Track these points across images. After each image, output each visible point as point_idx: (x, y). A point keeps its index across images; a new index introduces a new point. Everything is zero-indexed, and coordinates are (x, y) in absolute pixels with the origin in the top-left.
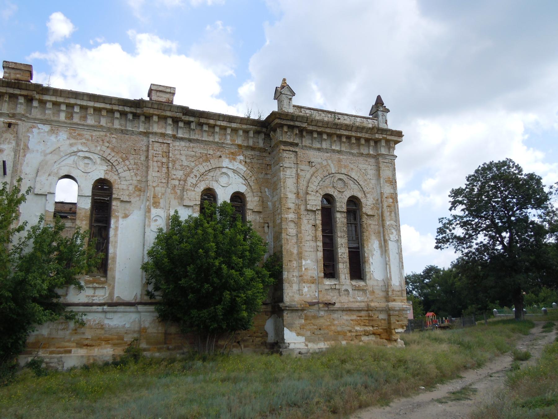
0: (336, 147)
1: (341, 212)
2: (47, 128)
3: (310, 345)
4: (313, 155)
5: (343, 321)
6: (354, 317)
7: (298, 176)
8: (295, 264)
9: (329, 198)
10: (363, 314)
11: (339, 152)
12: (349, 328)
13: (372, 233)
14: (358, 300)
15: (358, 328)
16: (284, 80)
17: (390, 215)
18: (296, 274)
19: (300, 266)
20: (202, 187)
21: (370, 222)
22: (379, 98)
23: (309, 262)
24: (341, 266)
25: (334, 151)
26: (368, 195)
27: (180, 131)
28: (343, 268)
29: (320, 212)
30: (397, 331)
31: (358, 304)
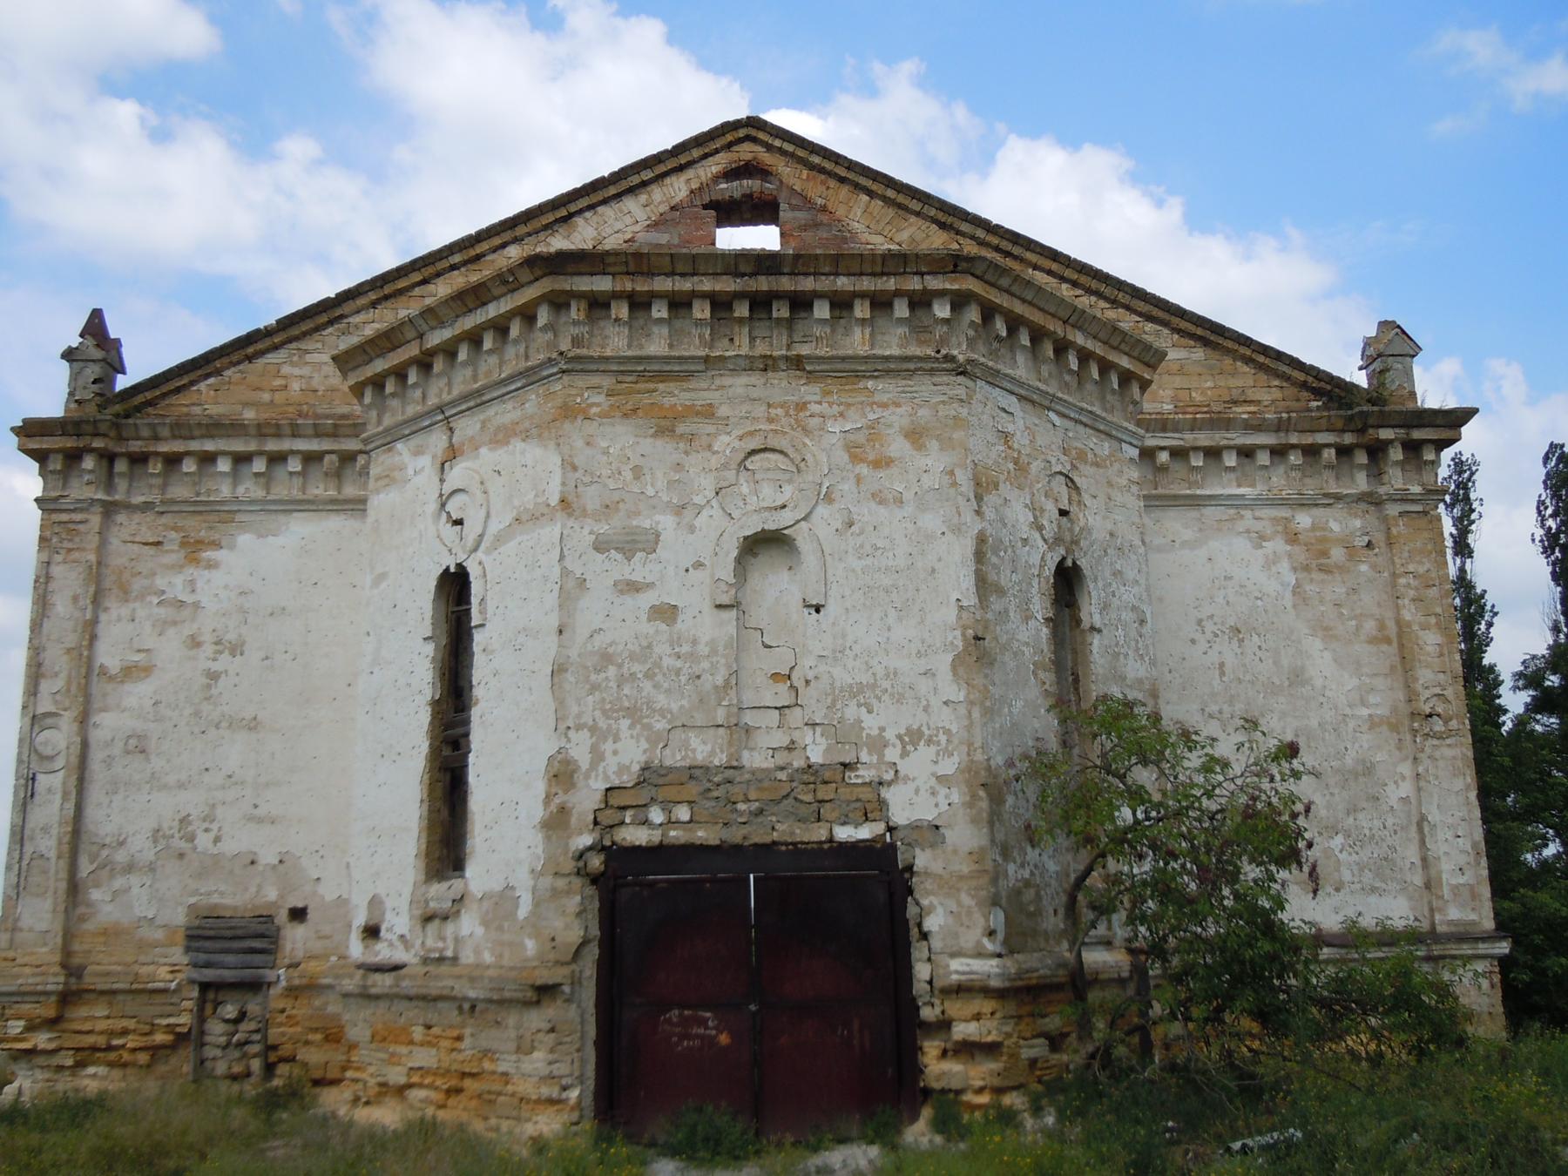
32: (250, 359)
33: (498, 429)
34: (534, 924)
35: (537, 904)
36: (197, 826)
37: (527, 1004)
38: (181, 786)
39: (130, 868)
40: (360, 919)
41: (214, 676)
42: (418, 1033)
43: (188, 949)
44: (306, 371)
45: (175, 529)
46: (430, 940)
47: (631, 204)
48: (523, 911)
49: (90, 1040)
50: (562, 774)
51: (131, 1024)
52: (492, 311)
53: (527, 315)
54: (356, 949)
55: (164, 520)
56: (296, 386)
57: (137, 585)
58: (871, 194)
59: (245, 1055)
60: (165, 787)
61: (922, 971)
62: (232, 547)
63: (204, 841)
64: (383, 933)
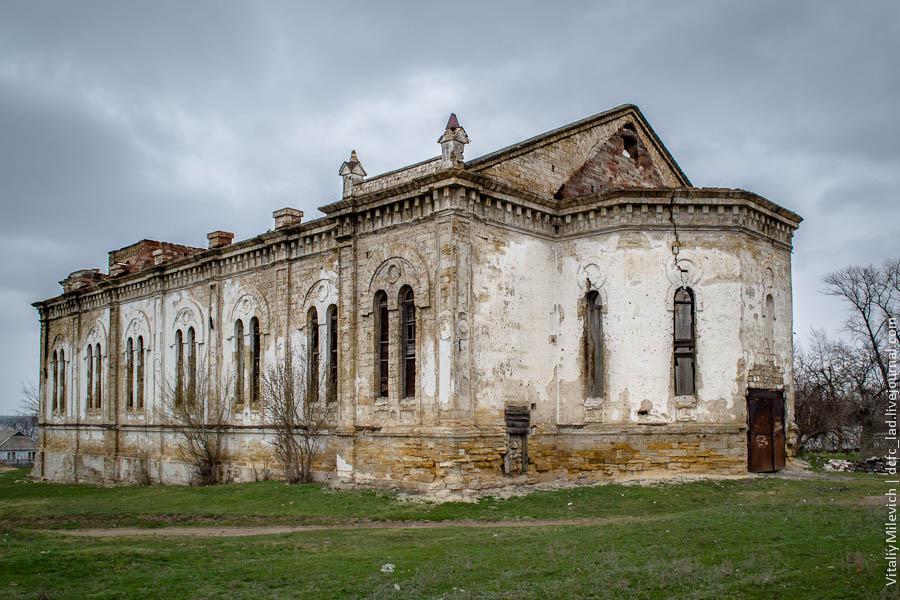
2: (229, 281)
3: (359, 476)
4: (370, 243)
7: (355, 275)
10: (411, 441)
11: (395, 227)
14: (403, 423)
15: (406, 459)
16: (354, 152)
17: (445, 302)
19: (353, 386)
21: (426, 316)
23: (363, 379)
25: (407, 224)
26: (421, 280)
27: (294, 251)
28: (394, 384)
30: (442, 465)
31: (403, 429)
34: (734, 410)
35: (735, 404)
36: (505, 368)
38: (500, 351)
39: (487, 385)
40: (638, 408)
41: (506, 303)
42: (675, 445)
43: (506, 420)
45: (493, 234)
46: (681, 415)
47: (605, 128)
50: (741, 364)
51: (490, 450)
52: (714, 201)
53: (728, 208)
54: (635, 418)
55: (487, 228)
56: (522, 176)
57: (482, 256)
58: (657, 149)
59: (517, 462)
62: (509, 246)
63: (508, 374)
64: (652, 412)
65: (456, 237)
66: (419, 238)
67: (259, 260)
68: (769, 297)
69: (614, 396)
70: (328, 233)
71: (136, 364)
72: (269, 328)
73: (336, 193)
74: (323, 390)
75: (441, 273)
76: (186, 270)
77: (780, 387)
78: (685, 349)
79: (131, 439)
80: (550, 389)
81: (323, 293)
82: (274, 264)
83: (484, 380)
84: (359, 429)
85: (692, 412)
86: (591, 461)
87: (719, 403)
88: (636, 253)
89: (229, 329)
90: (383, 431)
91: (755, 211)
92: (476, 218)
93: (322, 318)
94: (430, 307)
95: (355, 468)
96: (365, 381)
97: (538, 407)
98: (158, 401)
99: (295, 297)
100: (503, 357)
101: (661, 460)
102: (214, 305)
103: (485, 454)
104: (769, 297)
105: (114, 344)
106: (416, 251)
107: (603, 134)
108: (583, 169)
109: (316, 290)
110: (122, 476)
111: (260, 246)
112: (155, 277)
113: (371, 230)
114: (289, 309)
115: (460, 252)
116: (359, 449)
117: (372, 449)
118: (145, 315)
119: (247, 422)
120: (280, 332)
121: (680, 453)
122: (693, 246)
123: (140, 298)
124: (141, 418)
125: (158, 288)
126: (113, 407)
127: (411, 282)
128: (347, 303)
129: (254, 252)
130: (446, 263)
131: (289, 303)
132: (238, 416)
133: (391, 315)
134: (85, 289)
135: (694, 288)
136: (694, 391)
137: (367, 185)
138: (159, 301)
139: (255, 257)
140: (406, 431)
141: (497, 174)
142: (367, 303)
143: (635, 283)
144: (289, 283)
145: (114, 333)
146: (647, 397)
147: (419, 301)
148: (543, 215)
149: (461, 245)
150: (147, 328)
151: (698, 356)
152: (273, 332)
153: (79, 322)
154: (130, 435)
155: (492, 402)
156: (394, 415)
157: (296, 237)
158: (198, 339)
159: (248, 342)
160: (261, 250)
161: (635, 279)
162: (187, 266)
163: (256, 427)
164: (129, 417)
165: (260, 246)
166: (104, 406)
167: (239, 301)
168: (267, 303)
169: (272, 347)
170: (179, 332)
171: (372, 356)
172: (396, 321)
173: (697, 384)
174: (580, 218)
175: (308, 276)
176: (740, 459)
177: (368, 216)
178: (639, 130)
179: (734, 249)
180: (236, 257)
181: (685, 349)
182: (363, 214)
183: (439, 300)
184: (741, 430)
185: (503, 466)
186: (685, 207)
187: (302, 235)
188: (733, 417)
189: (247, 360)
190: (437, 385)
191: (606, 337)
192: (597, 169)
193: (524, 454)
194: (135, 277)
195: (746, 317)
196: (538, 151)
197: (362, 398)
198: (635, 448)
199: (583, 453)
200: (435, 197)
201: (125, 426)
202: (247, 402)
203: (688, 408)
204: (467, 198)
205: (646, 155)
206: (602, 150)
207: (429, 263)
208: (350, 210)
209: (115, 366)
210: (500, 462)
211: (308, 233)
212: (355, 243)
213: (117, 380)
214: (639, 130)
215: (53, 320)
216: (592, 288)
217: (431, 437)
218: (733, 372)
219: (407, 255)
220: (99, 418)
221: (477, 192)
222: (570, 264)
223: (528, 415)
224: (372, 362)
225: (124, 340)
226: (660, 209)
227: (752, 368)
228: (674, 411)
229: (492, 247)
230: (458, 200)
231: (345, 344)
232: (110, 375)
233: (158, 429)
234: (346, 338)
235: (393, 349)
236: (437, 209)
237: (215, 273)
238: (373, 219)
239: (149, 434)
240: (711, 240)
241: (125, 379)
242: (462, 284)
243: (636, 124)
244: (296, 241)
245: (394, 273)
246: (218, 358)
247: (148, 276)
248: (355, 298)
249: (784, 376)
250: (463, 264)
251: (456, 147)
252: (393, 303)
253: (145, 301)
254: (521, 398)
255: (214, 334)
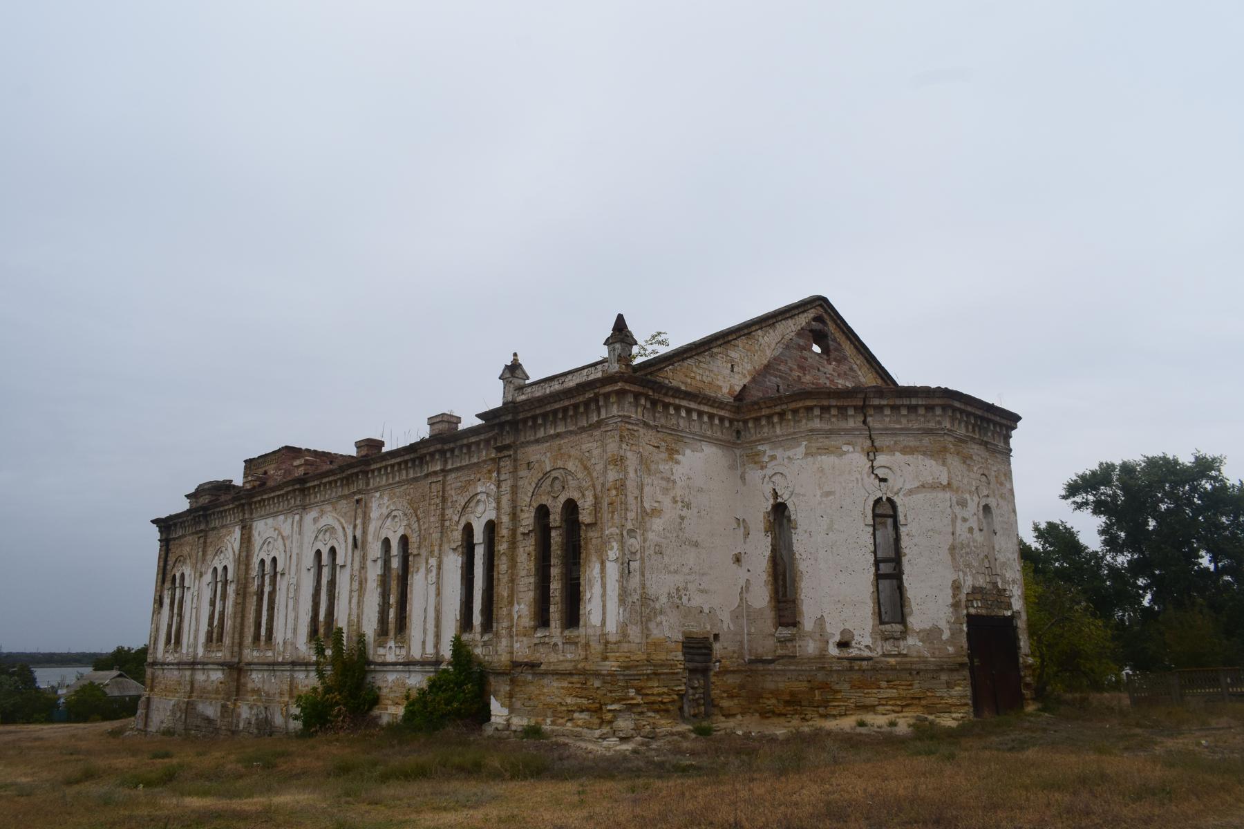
0: (561, 429)
1: (555, 528)
2: (378, 494)
5: (553, 689)
6: (565, 684)
7: (514, 489)
8: (504, 611)
9: (543, 512)
10: (575, 679)
11: (558, 435)
12: (559, 700)
13: (593, 552)
14: (567, 657)
15: (569, 700)
16: (515, 355)
18: (505, 625)
19: (510, 614)
20: (463, 523)
22: (620, 319)
24: (552, 609)
25: (571, 432)
26: (586, 493)
27: (450, 462)
29: (532, 534)
32: (683, 360)
33: (905, 447)
34: (951, 641)
35: (952, 634)
36: (682, 592)
37: (952, 670)
40: (837, 638)
41: (682, 518)
42: (884, 684)
43: (684, 654)
44: (701, 371)
46: (888, 647)
47: (791, 322)
48: (946, 635)
49: (652, 698)
50: (956, 587)
51: (665, 690)
52: (914, 402)
54: (833, 651)
55: (660, 435)
57: (653, 467)
60: (670, 572)
61: (1021, 660)
63: (685, 599)
64: (853, 643)
65: (624, 446)
66: (584, 447)
67: (411, 471)
68: (987, 509)
69: (808, 624)
70: (487, 442)
71: (267, 589)
72: (419, 548)
73: (494, 398)
74: (477, 619)
75: (608, 485)
76: (330, 483)
77: (1009, 613)
78: (889, 570)
79: (256, 678)
80: (736, 616)
81: (481, 508)
82: (427, 476)
83: (658, 607)
84: (515, 664)
85: (902, 643)
86: (787, 703)
87: (931, 634)
88: (827, 460)
89: (375, 550)
90: (543, 667)
91: (962, 412)
92: (646, 425)
93: (479, 537)
94: (595, 524)
95: (511, 712)
96: (523, 609)
97: (721, 638)
98: (289, 635)
99: (449, 512)
100: (678, 580)
101: (868, 701)
102: (359, 522)
103: (659, 695)
104: (987, 509)
105: (243, 567)
106: (581, 461)
107: (789, 328)
108: (767, 367)
109: (472, 504)
110: (241, 726)
111: (412, 456)
112: (294, 490)
113: (532, 438)
114: (443, 525)
115: (628, 462)
116: (517, 689)
117: (533, 689)
118: (280, 533)
119: (391, 658)
120: (432, 552)
121: (893, 693)
122: (891, 451)
123: (275, 515)
124: (270, 654)
125: (298, 502)
126: (237, 641)
127: (575, 495)
128: (505, 519)
129: (406, 462)
130: (612, 475)
131: (443, 518)
132: (381, 651)
133: (553, 533)
134: (214, 504)
135: (895, 499)
136: (903, 620)
137: (529, 390)
138: (297, 517)
139: (392, 472)
140: (568, 667)
141: (674, 377)
142: (528, 519)
143: (828, 494)
144: (443, 497)
145: (244, 554)
146: (847, 627)
147: (585, 517)
148: (722, 419)
149: (629, 454)
150: (281, 548)
151: (904, 577)
152: (424, 552)
153: (205, 542)
154: (254, 675)
155: (669, 629)
156: (556, 648)
157: (452, 445)
158: (339, 561)
159: (395, 563)
160: (413, 460)
161: (826, 489)
162: (331, 478)
163: (400, 664)
164: (255, 653)
165: (412, 456)
166: (227, 640)
167: (387, 517)
168: (418, 520)
169: (422, 570)
170: (319, 553)
171: (532, 580)
172: (559, 539)
173: (907, 610)
174: (764, 422)
175: (463, 489)
176: (963, 701)
177: (530, 423)
178: (829, 322)
179: (939, 454)
180: (386, 467)
181: (889, 570)
182: (525, 421)
183: (606, 516)
184: (962, 665)
185: (681, 709)
186: (880, 408)
187: (459, 443)
188: (951, 649)
189: (394, 585)
190: (604, 614)
191: (797, 556)
192: (782, 367)
193: (707, 694)
194: (273, 489)
195: (958, 532)
196: (715, 350)
197: (520, 628)
198: (837, 687)
199: (776, 693)
200: (601, 403)
201: (249, 664)
202: (392, 634)
203: (898, 639)
204: (637, 404)
205: (839, 348)
206: (787, 347)
207: (595, 474)
208: (509, 418)
209: (242, 593)
210: (679, 704)
211: (465, 441)
212: (516, 452)
213: (243, 611)
214: (829, 322)
215: (175, 539)
216: (780, 500)
217: (597, 674)
218: (947, 597)
219: (571, 466)
220: (219, 654)
221: (647, 397)
222: (754, 475)
223: (710, 649)
224: (532, 587)
225: (255, 562)
226: (851, 412)
227: (969, 591)
228: (879, 643)
229: (664, 456)
230: (626, 405)
231: (502, 565)
232: (236, 604)
233: (287, 667)
234: (504, 559)
235: (555, 571)
236: (603, 415)
237: (361, 484)
238: (535, 427)
239: (278, 673)
240: (911, 444)
241: (253, 608)
242: (631, 499)
243: (825, 316)
244: (452, 450)
245: (557, 485)
246: (361, 583)
247: (286, 490)
248: (514, 514)
249: (1013, 600)
250: (632, 474)
251: (623, 350)
252: (555, 519)
253: (282, 518)
254: (699, 628)
255: (358, 553)
